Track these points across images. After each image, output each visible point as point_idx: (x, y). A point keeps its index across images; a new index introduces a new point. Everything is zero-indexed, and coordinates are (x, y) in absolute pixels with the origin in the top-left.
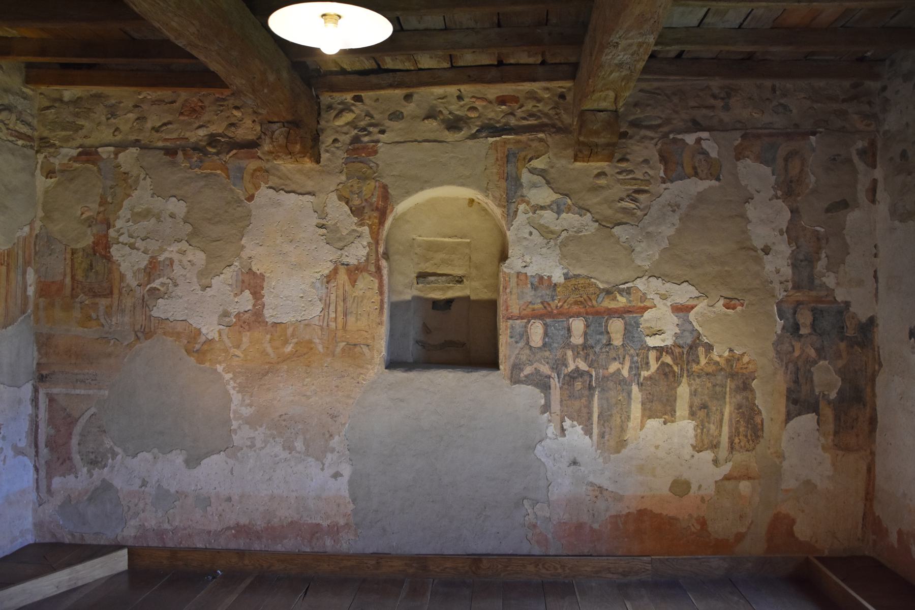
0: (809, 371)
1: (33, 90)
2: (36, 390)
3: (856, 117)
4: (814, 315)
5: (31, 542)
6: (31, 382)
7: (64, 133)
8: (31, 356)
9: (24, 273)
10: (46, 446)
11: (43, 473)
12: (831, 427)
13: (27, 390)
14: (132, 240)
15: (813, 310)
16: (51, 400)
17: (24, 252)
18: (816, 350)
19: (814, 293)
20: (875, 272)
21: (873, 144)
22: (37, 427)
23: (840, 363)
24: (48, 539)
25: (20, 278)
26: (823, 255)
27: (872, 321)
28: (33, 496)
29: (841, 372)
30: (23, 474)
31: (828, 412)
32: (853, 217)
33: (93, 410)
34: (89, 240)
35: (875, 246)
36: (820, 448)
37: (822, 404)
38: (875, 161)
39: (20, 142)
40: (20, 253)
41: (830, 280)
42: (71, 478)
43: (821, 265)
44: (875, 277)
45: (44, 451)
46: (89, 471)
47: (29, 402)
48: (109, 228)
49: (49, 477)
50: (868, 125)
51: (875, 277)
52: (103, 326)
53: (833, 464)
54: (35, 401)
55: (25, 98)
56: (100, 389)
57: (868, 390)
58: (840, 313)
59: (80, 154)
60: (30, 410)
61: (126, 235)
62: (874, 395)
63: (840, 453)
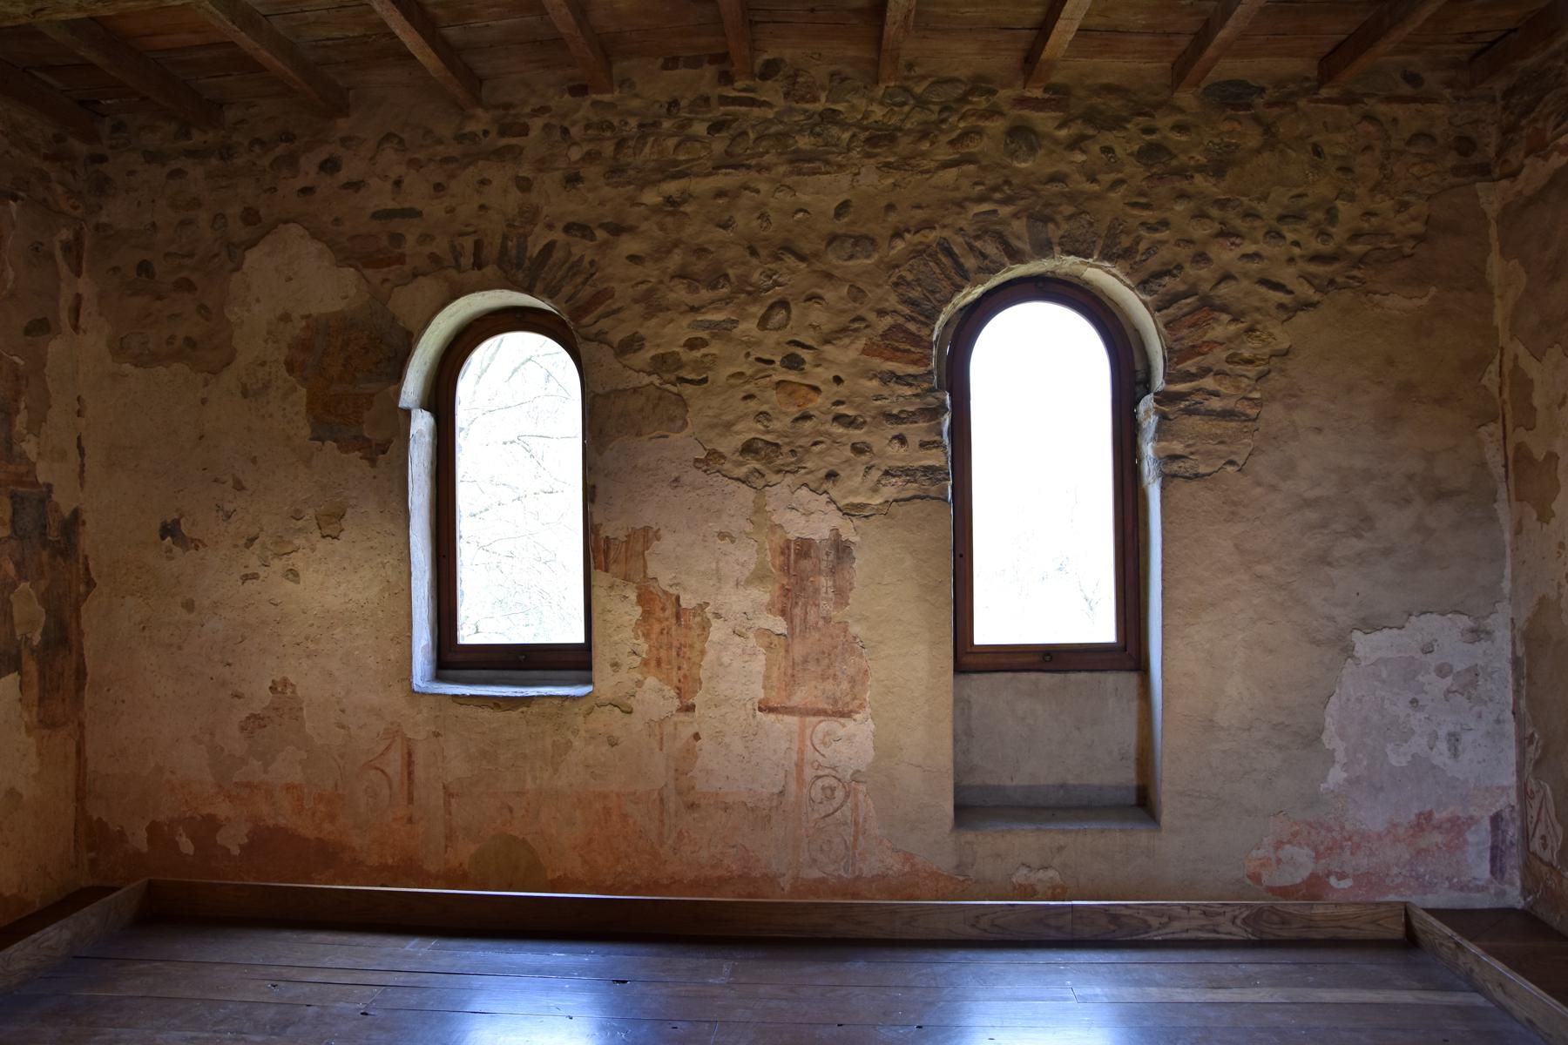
0: (9, 601)
3: (60, 189)
4: (14, 504)
12: (34, 693)
15: (13, 496)
18: (18, 565)
19: (12, 468)
20: (79, 439)
21: (78, 238)
23: (43, 585)
26: (22, 406)
27: (76, 513)
29: (44, 599)
31: (31, 667)
32: (55, 347)
35: (79, 399)
36: (23, 729)
37: (25, 655)
38: (79, 265)
41: (30, 447)
43: (21, 421)
44: (80, 447)
50: (75, 208)
51: (80, 447)
53: (39, 754)
57: (74, 625)
58: (42, 501)
62: (81, 633)
63: (46, 732)
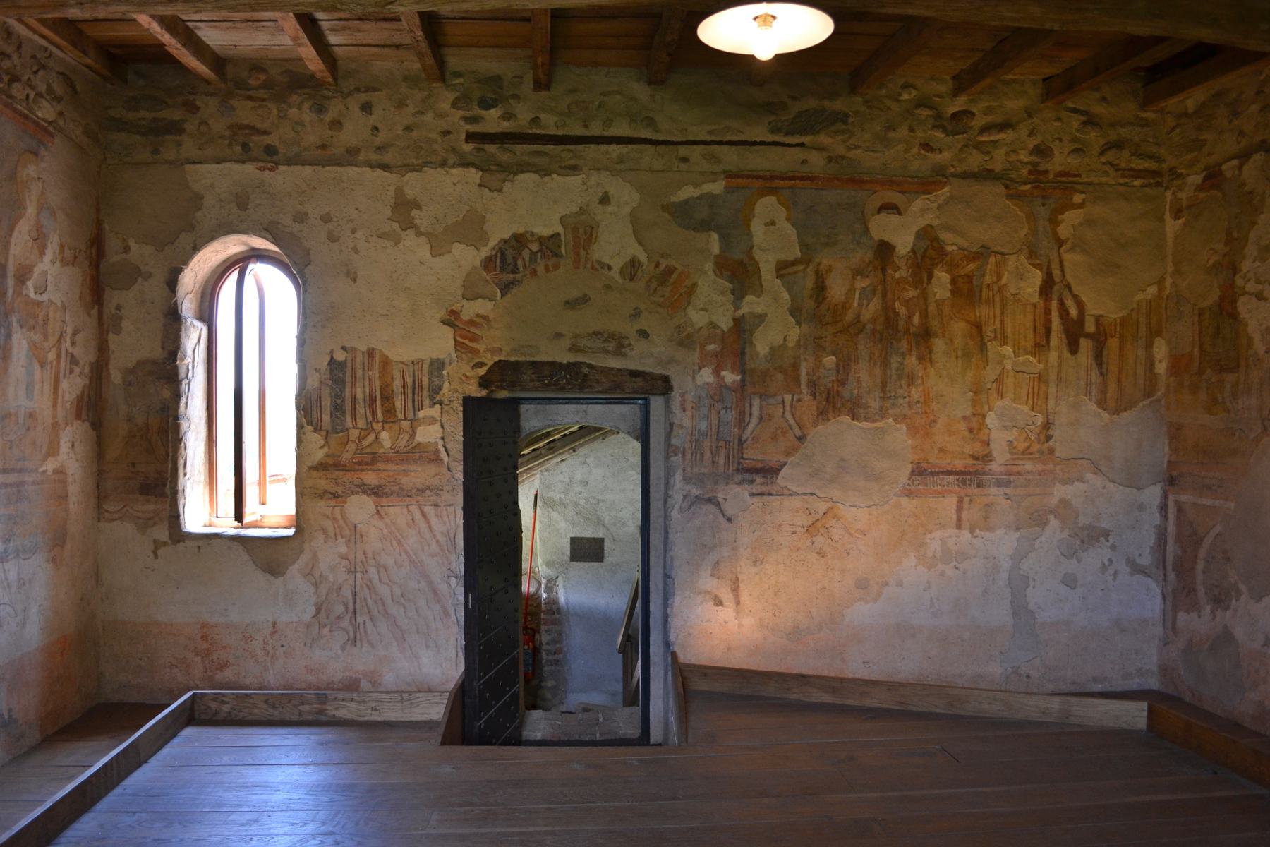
1: (1155, 112)
2: (1165, 496)
5: (1155, 688)
6: (1159, 486)
7: (1189, 156)
8: (1161, 451)
9: (1149, 346)
10: (1174, 569)
11: (1169, 603)
13: (1153, 494)
14: (1260, 287)
16: (1180, 510)
17: (1148, 317)
22: (1166, 543)
24: (1170, 691)
25: (1141, 353)
28: (1159, 630)
30: (1148, 600)
33: (1218, 529)
34: (1215, 295)
39: (1137, 182)
40: (1142, 320)
42: (1194, 615)
45: (1172, 576)
46: (1212, 612)
47: (1155, 510)
48: (1235, 274)
49: (1175, 609)
52: (1229, 412)
54: (1163, 509)
55: (1143, 126)
56: (1226, 500)
59: (1205, 179)
60: (1157, 520)
61: (1252, 282)
